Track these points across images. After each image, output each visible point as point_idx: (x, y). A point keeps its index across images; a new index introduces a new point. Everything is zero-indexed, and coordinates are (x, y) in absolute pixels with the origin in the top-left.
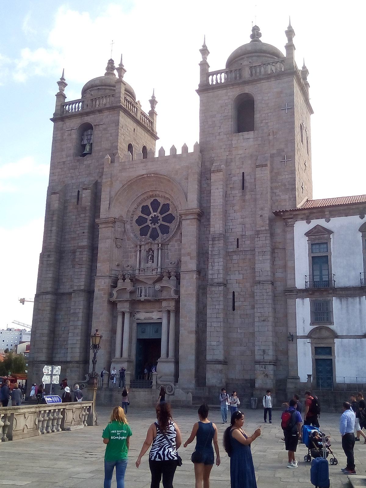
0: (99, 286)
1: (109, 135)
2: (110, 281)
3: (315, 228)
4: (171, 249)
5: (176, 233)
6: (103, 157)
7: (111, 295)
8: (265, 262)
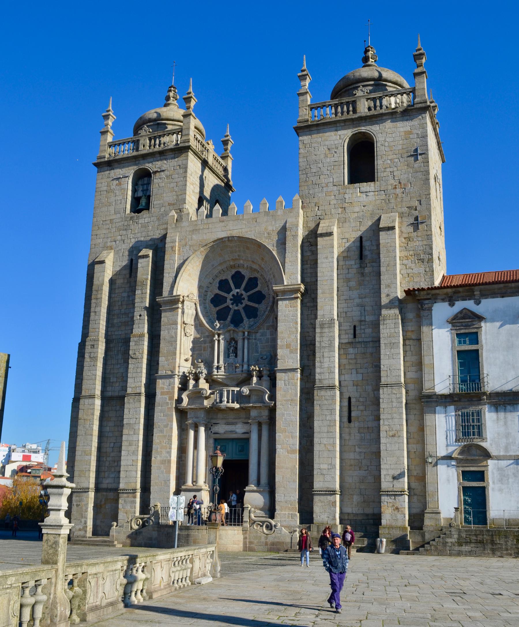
0: (163, 388)
1: (172, 185)
3: (461, 312)
4: (261, 339)
5: (268, 317)
6: (166, 214)
7: (180, 400)
8: (394, 357)
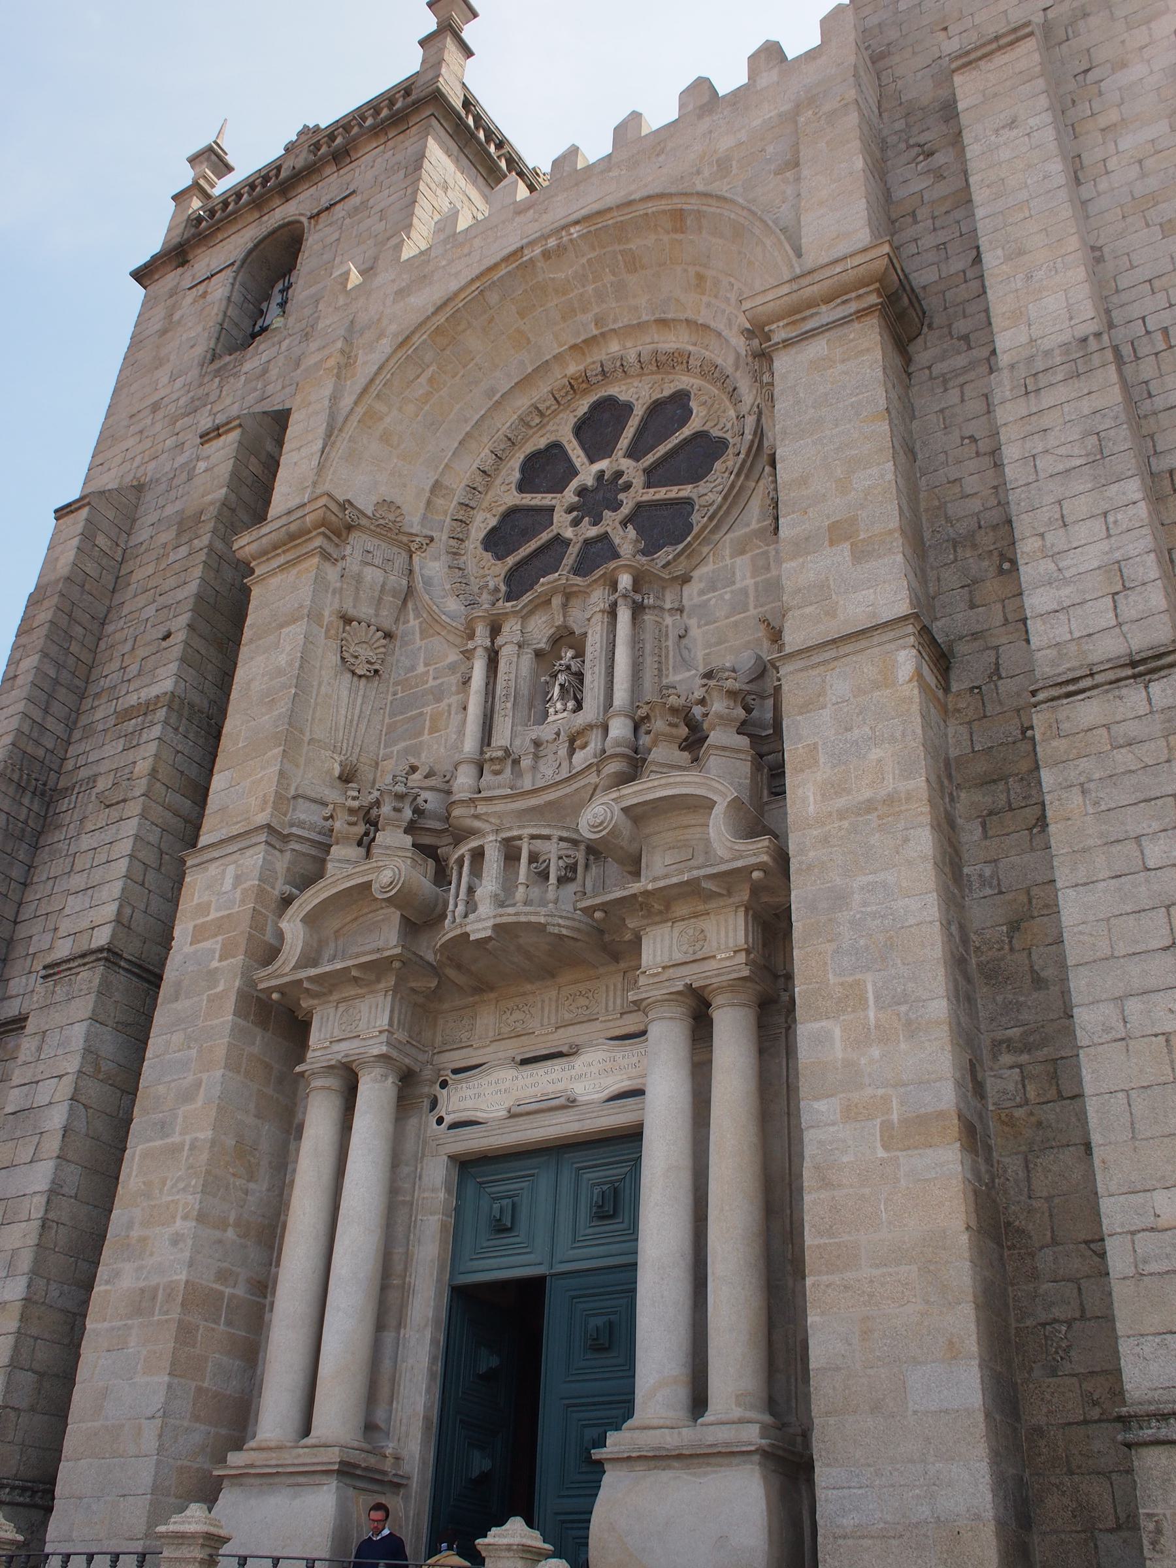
0: (204, 908)
2: (282, 863)
4: (704, 605)
7: (270, 954)
